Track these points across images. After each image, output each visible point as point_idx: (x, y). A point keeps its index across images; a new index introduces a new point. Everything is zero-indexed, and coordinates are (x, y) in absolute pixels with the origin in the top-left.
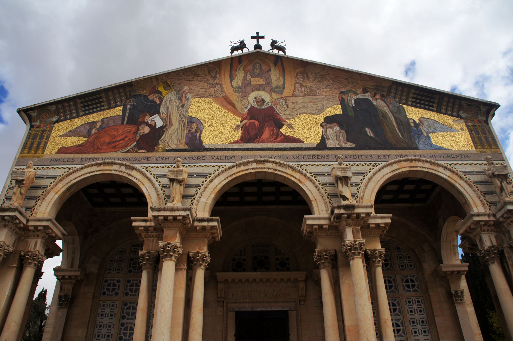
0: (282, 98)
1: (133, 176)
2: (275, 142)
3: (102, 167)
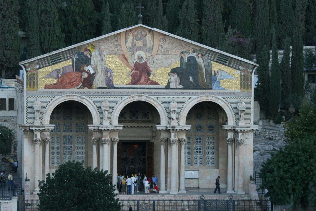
1: (84, 102)
2: (146, 85)
3: (68, 97)
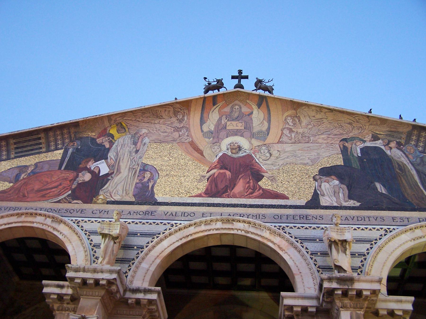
0: (265, 145)
1: (58, 231)
2: (250, 198)
